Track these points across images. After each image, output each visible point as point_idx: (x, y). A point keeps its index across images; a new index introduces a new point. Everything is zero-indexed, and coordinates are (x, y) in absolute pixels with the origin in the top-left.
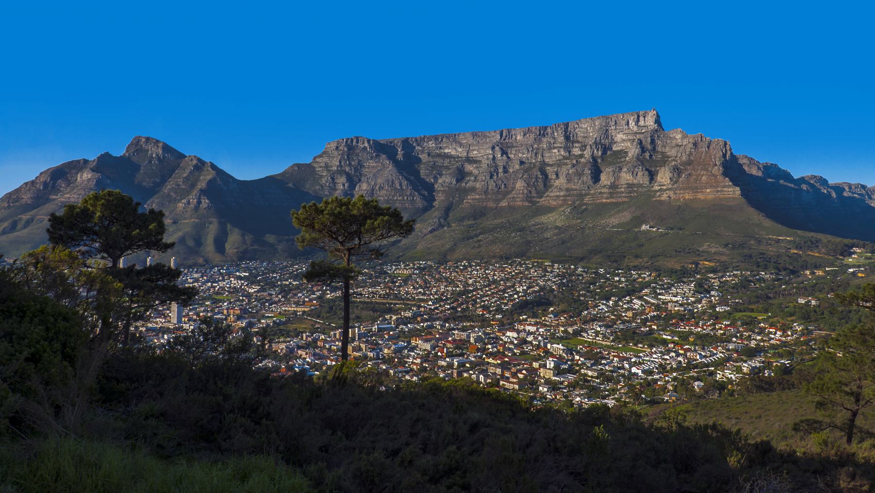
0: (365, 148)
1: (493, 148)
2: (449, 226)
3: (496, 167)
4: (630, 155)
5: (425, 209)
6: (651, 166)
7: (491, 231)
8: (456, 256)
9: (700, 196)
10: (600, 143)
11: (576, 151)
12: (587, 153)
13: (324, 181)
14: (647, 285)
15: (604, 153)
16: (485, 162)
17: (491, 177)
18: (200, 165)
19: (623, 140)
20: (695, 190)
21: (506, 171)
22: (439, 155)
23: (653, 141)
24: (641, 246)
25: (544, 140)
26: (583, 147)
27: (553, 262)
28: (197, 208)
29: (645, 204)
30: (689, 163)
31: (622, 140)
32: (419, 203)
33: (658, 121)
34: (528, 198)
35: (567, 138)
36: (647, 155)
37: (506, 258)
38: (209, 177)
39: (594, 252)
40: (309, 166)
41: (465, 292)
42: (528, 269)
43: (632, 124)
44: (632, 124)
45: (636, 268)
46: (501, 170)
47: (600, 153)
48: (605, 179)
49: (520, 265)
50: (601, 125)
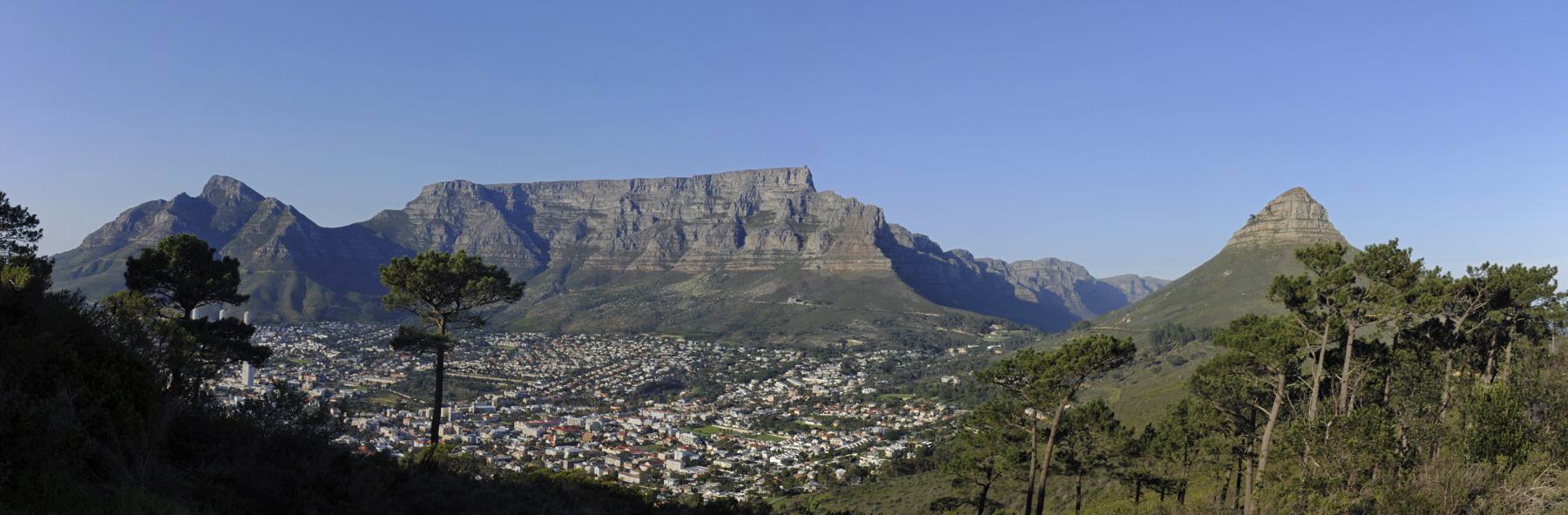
0: (468, 195)
1: (622, 201)
2: (565, 291)
3: (625, 223)
4: (778, 216)
5: (538, 271)
7: (615, 299)
8: (572, 327)
9: (851, 267)
11: (719, 209)
12: (731, 213)
13: (418, 231)
14: (790, 366)
15: (750, 213)
16: (612, 217)
18: (280, 208)
20: (846, 260)
21: (636, 228)
22: (556, 207)
23: (803, 202)
24: (785, 321)
25: (683, 194)
26: (727, 205)
27: (687, 339)
28: (274, 257)
29: (792, 273)
30: (841, 229)
31: (772, 201)
32: (531, 263)
33: (809, 181)
34: (661, 262)
35: (709, 193)
36: (797, 218)
37: (632, 333)
38: (288, 223)
39: (735, 327)
40: (402, 212)
41: (581, 371)
42: (657, 346)
43: (782, 181)
45: (780, 347)
46: (630, 227)
48: (750, 242)
49: (648, 340)
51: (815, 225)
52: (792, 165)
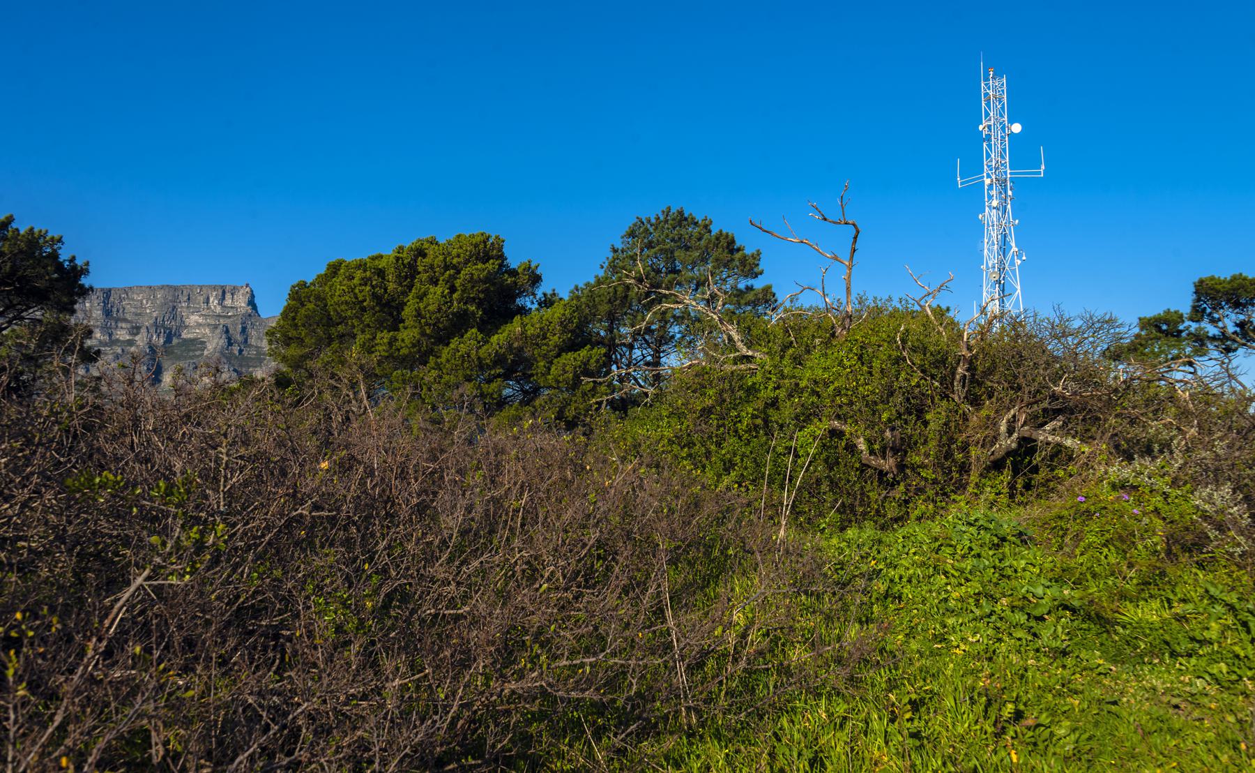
4: (210, 347)
6: (241, 366)
10: (163, 326)
12: (141, 340)
15: (169, 339)
19: (199, 325)
23: (244, 330)
26: (135, 330)
31: (195, 324)
33: (252, 303)
35: (107, 313)
36: (236, 349)
43: (214, 302)
44: (214, 302)
47: (162, 340)
50: (165, 298)
52: (229, 282)
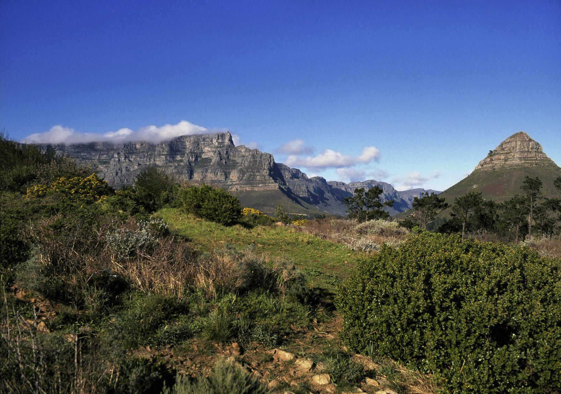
6: (226, 169)
10: (194, 153)
15: (196, 159)
17: (117, 174)
36: (224, 161)
51: (234, 165)
